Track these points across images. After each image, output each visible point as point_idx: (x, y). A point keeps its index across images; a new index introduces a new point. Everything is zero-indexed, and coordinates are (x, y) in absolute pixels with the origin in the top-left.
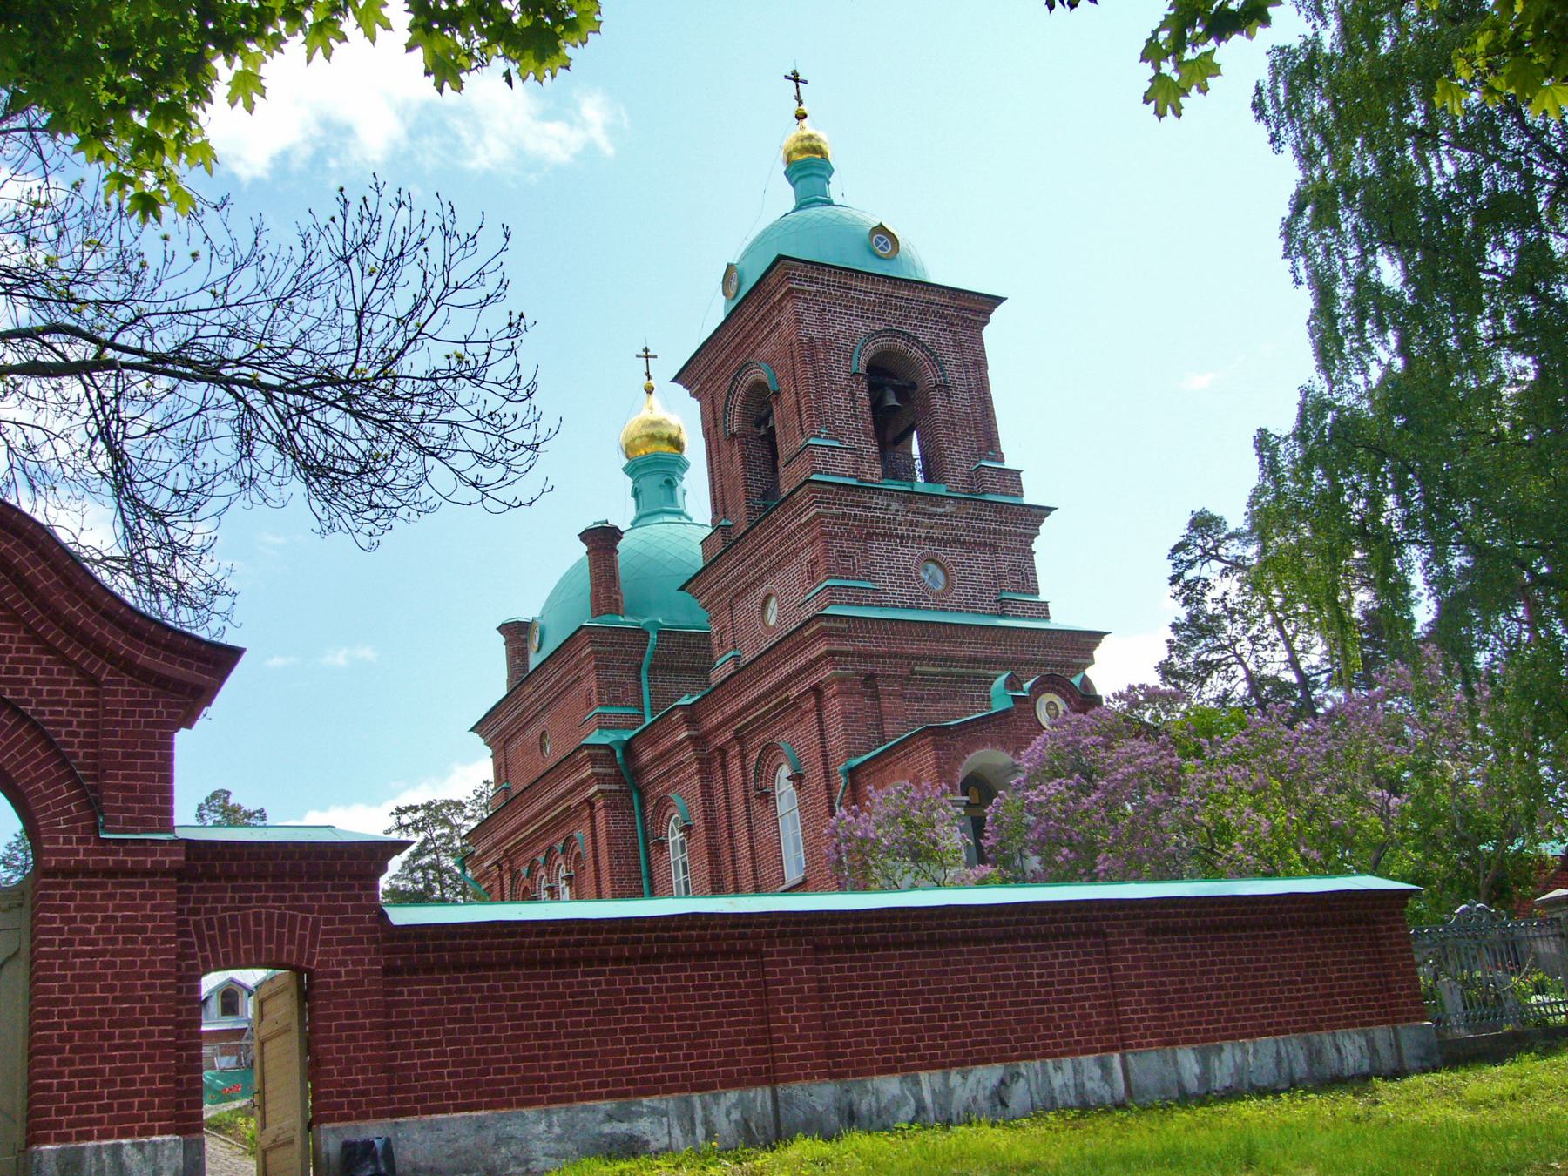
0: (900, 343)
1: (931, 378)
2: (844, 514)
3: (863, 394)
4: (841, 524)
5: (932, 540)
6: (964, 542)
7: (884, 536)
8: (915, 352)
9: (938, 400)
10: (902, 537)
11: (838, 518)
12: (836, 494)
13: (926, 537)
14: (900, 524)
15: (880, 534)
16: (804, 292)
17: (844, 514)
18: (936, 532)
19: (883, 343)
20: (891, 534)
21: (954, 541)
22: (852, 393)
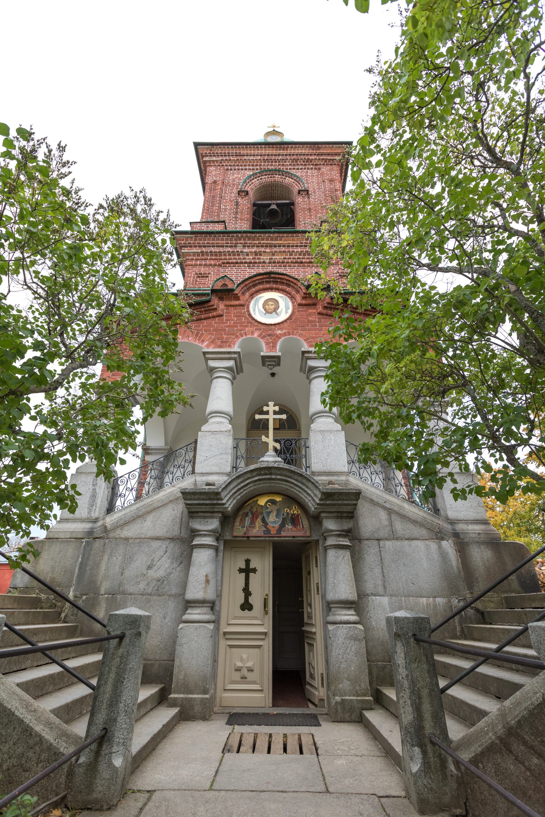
0: (278, 178)
1: (296, 188)
2: (202, 252)
3: (246, 204)
4: (203, 260)
5: (274, 263)
6: (301, 263)
7: (237, 263)
8: (288, 180)
9: (299, 200)
10: (250, 263)
11: (198, 255)
12: (196, 240)
13: (270, 263)
14: (247, 255)
15: (232, 263)
16: (213, 161)
17: (202, 252)
18: (277, 258)
19: (266, 179)
20: (241, 263)
21: (292, 262)
22: (237, 202)
